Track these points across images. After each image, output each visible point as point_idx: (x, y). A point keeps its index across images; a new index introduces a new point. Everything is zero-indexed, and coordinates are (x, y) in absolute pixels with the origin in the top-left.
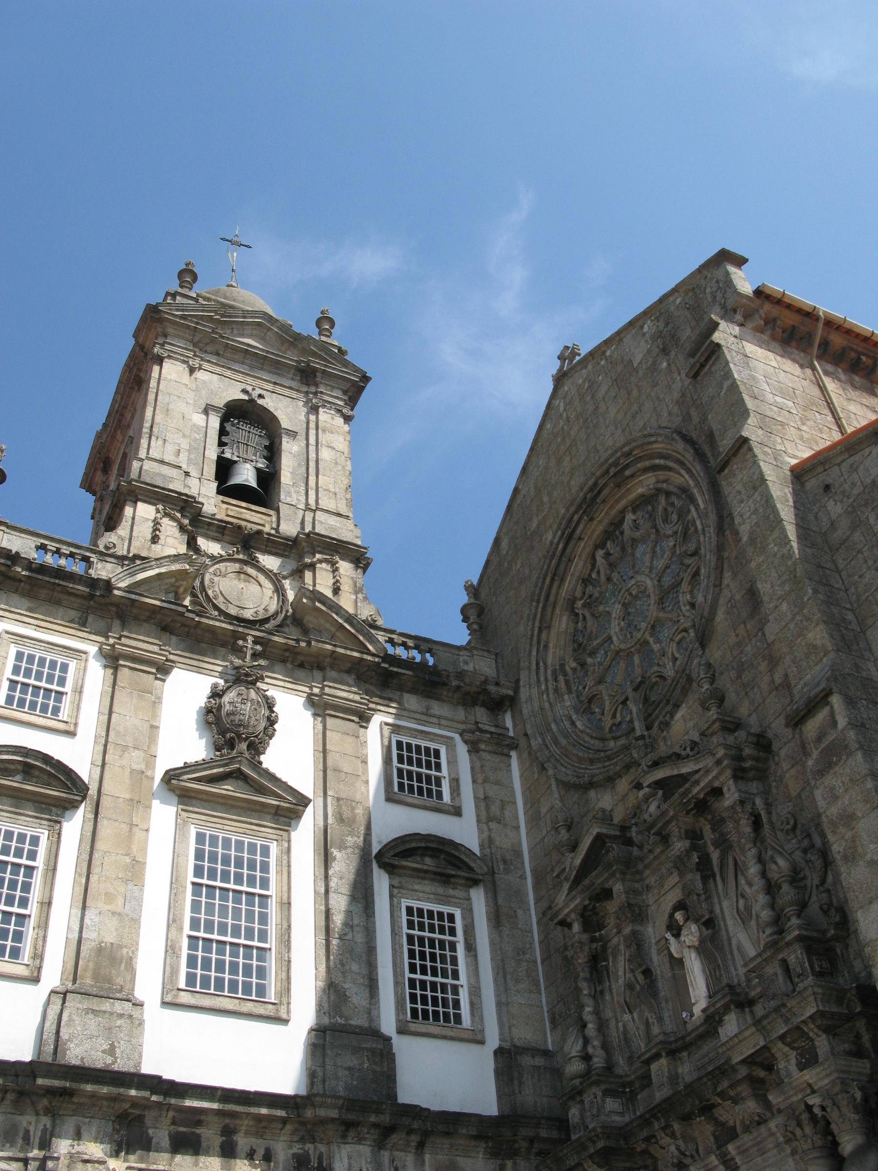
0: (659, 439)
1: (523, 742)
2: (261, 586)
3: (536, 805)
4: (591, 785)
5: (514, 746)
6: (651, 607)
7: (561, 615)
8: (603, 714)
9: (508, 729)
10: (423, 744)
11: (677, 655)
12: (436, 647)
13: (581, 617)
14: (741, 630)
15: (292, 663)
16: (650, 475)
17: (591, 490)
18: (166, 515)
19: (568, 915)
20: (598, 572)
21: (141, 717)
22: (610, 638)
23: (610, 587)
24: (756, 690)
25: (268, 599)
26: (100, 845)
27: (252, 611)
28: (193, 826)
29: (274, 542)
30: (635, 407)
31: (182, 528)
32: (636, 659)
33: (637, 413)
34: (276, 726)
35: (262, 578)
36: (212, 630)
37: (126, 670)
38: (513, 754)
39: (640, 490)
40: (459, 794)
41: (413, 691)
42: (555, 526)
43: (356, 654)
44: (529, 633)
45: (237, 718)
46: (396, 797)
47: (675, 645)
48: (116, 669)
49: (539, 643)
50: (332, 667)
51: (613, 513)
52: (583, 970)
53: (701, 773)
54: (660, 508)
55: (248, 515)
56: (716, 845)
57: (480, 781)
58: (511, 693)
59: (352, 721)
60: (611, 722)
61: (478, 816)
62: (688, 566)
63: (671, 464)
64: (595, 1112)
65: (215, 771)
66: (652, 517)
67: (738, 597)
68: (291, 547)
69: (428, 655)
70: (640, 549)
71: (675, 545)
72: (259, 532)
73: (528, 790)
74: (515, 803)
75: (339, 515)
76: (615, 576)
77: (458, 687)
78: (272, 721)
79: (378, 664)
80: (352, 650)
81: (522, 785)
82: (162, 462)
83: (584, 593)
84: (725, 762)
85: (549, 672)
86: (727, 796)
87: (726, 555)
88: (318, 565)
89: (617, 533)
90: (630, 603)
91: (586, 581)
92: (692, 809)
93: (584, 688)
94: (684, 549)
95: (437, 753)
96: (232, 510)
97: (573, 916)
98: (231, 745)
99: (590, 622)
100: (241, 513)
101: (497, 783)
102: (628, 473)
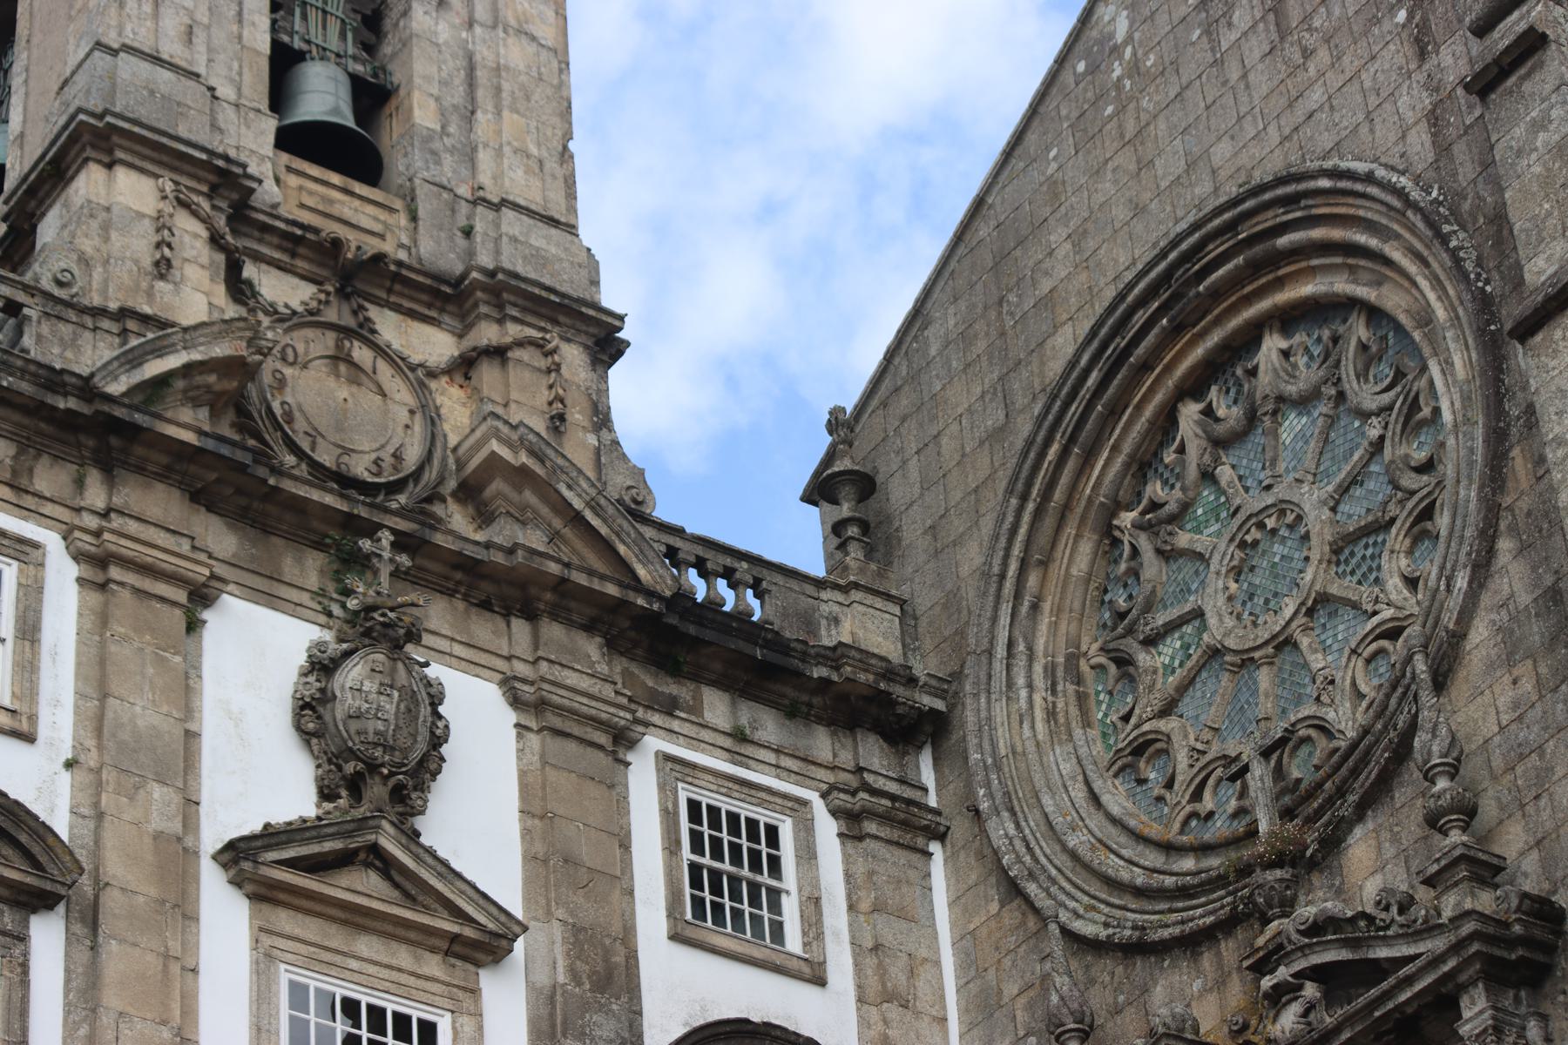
0: (1373, 190)
1: (960, 828)
2: (384, 395)
3: (992, 973)
4: (1138, 949)
5: (941, 837)
7: (1078, 537)
8: (1169, 785)
9: (925, 790)
10: (745, 811)
11: (1363, 688)
12: (769, 578)
13: (1127, 548)
14: (1524, 669)
15: (466, 598)
16: (1338, 260)
17: (1186, 258)
18: (184, 204)
20: (1181, 450)
21: (165, 709)
22: (1198, 614)
23: (1208, 494)
24: (1543, 802)
25: (400, 430)
26: (112, 999)
27: (368, 459)
28: (283, 966)
29: (407, 282)
31: (215, 240)
32: (1264, 677)
34: (445, 750)
35: (384, 371)
36: (299, 506)
37: (126, 594)
38: (935, 847)
40: (820, 936)
41: (723, 683)
42: (1085, 326)
43: (612, 590)
44: (996, 570)
45: (374, 726)
46: (690, 932)
47: (1360, 663)
48: (103, 586)
49: (1018, 595)
50: (558, 614)
51: (1235, 322)
53: (1419, 963)
54: (1353, 342)
55: (347, 208)
57: (865, 906)
58: (940, 705)
59: (600, 747)
60: (1188, 809)
61: (859, 987)
62: (1413, 493)
63: (1397, 256)
65: (328, 846)
66: (1330, 355)
67: (1524, 599)
68: (447, 298)
69: (721, 584)
70: (1293, 425)
71: (1382, 438)
72: (379, 258)
73: (965, 939)
74: (938, 964)
75: (553, 222)
76: (1225, 473)
77: (826, 682)
78: (438, 740)
79: (657, 616)
80: (603, 577)
81: (953, 924)
82: (156, 60)
83: (1139, 495)
84: (1475, 947)
85: (1038, 669)
86: (1466, 1014)
87: (1507, 501)
88: (515, 354)
89: (1239, 372)
90: (1256, 543)
91: (1143, 466)
92: (1388, 1032)
93: (1126, 718)
94: (1402, 450)
95: (773, 833)
96: (311, 193)
98: (355, 786)
99: (1151, 566)
100: (331, 202)
101: (903, 914)
102: (1283, 241)
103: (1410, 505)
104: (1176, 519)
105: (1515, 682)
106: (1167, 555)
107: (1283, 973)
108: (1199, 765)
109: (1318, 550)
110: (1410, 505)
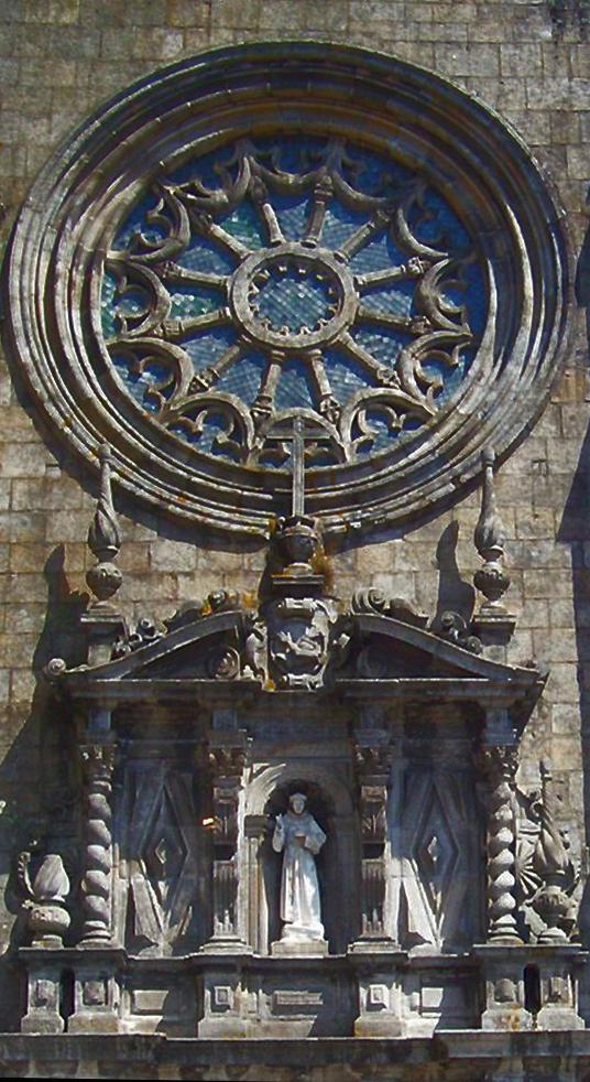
6: (338, 322)
8: (168, 392)
11: (364, 426)
19: (105, 699)
22: (220, 296)
24: (541, 605)
30: (459, 34)
32: (275, 370)
33: (458, 45)
39: (394, 145)
42: (199, 45)
52: (104, 790)
54: (413, 197)
56: (408, 753)
62: (438, 327)
63: (493, 181)
64: (100, 996)
93: (134, 323)
97: (114, 704)
103: (437, 334)
104: (220, 214)
105: (536, 516)
106: (202, 237)
107: (309, 603)
108: (197, 397)
109: (347, 315)
110: (437, 334)
